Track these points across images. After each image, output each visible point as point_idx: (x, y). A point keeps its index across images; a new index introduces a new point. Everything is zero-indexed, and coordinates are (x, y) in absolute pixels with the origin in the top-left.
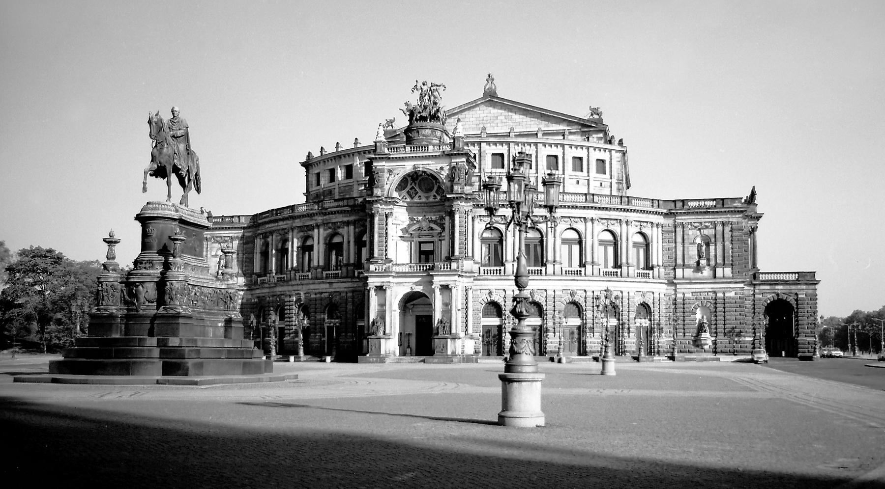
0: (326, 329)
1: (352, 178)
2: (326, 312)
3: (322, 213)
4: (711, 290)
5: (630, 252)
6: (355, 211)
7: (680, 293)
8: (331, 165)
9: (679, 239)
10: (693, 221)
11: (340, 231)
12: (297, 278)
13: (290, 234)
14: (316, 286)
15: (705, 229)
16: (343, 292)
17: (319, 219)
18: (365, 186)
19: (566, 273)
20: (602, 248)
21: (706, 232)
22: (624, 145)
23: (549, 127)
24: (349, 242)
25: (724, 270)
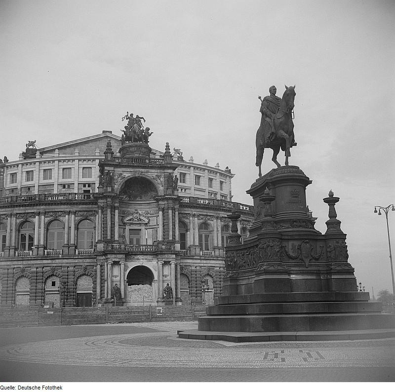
1: (50, 178)
16: (64, 267)
24: (69, 228)
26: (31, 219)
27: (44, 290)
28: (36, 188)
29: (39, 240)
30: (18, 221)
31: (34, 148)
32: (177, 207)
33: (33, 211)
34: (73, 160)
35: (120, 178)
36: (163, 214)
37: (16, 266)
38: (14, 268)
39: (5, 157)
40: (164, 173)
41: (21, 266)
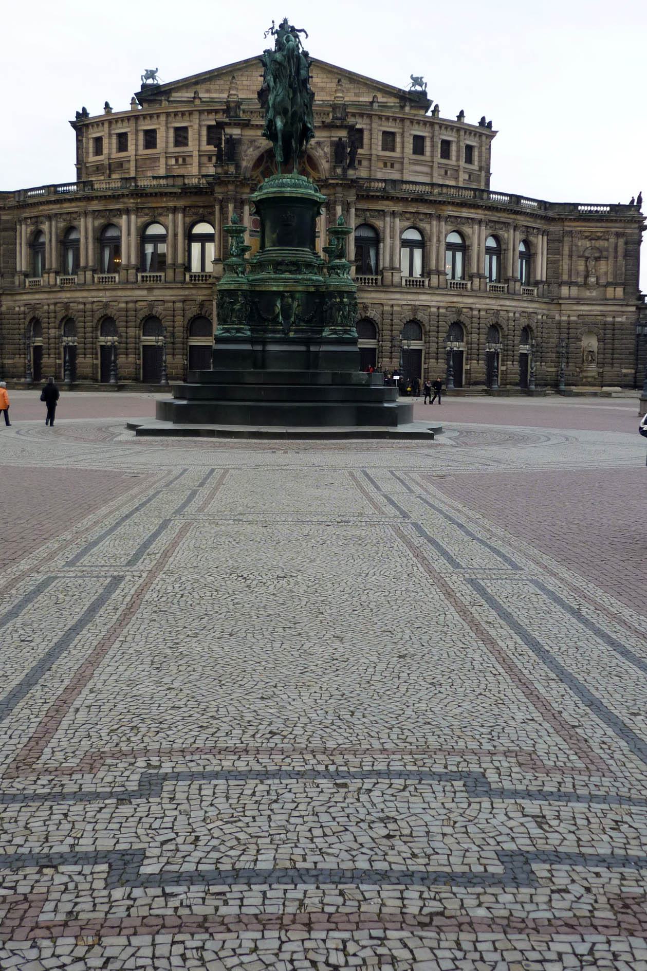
0: (141, 349)
2: (142, 327)
3: (137, 195)
4: (599, 313)
6: (186, 193)
7: (564, 315)
8: (120, 128)
9: (566, 251)
10: (583, 229)
11: (162, 219)
12: (96, 280)
13: (82, 220)
14: (128, 293)
17: (131, 202)
18: (177, 161)
22: (493, 129)
23: (359, 97)
24: (175, 235)
26: (115, 220)
27: (139, 338)
28: (133, 164)
29: (129, 257)
30: (97, 223)
31: (156, 82)
32: (352, 198)
33: (117, 207)
34: (191, 113)
35: (251, 149)
36: (328, 210)
37: (95, 299)
38: (93, 302)
39: (84, 109)
40: (330, 137)
41: (104, 300)
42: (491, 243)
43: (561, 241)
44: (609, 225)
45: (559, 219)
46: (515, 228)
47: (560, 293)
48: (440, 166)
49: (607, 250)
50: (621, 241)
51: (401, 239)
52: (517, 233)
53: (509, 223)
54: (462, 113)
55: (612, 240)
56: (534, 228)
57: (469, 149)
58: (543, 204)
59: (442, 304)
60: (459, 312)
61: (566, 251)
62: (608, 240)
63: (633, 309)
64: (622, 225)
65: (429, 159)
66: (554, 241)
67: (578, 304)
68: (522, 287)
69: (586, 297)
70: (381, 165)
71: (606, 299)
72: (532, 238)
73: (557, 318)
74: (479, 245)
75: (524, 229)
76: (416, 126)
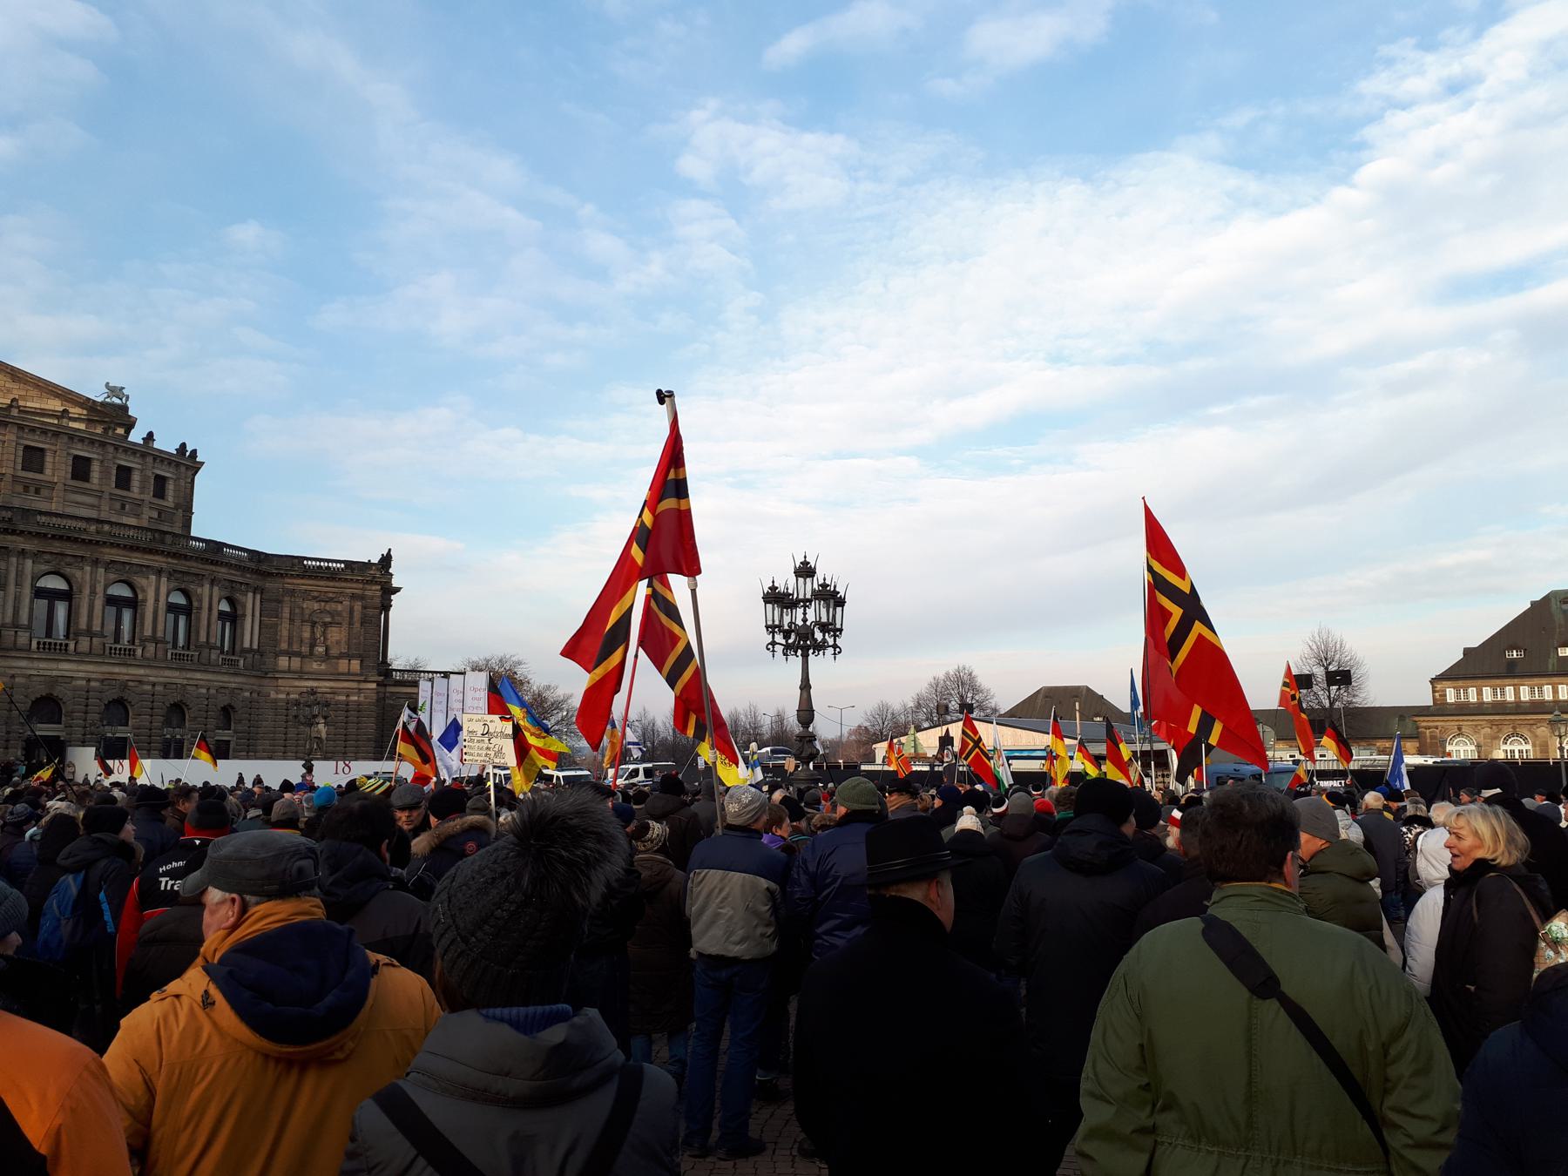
5: (213, 627)
7: (282, 692)
9: (286, 614)
15: (327, 602)
19: (110, 653)
20: (171, 617)
21: (330, 607)
22: (198, 460)
25: (349, 663)
42: (178, 599)
43: (279, 602)
44: (344, 584)
45: (277, 574)
46: (212, 583)
47: (276, 664)
48: (112, 497)
49: (339, 614)
50: (358, 606)
51: (33, 586)
52: (216, 589)
53: (203, 575)
54: (150, 435)
55: (347, 603)
56: (241, 583)
57: (160, 482)
58: (255, 555)
59: (94, 676)
60: (124, 686)
61: (286, 614)
62: (342, 603)
63: (374, 686)
64: (361, 586)
65: (97, 488)
66: (270, 601)
67: (301, 679)
68: (221, 656)
69: (312, 670)
70: (20, 488)
71: (339, 674)
72: (237, 596)
73: (273, 695)
74: (157, 600)
75: (227, 584)
76: (79, 446)
